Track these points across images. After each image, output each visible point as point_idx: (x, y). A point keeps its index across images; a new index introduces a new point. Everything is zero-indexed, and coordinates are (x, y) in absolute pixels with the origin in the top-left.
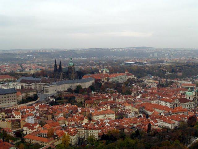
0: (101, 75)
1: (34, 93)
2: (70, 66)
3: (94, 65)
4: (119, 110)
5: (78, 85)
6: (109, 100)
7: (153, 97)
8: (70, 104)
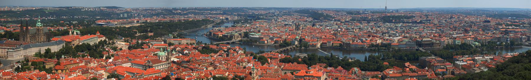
3: (64, 26)
4: (91, 76)
5: (47, 48)
6: (80, 65)
7: (124, 60)
8: (37, 71)
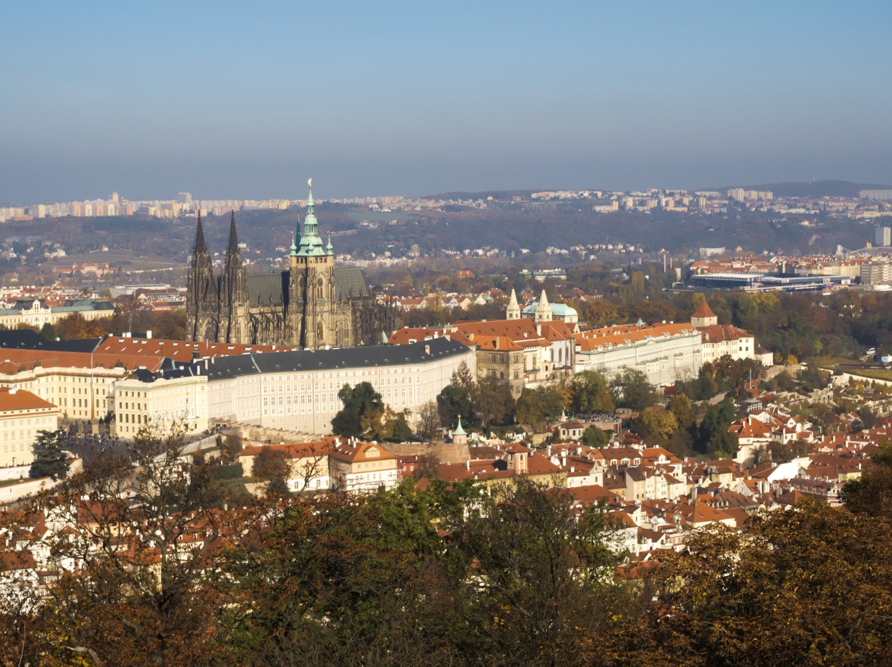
4: (645, 547)
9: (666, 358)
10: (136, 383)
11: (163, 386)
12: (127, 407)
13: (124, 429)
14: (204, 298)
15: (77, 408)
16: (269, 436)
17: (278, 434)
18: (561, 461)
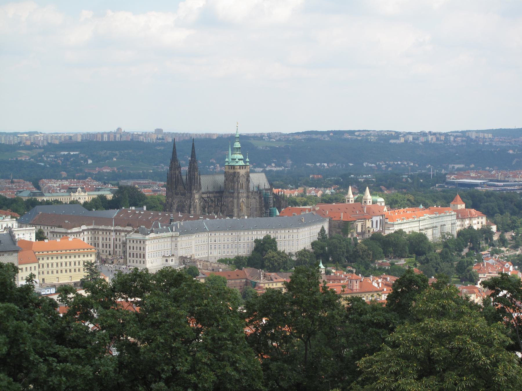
0: (353, 207)
1: (86, 259)
2: (233, 167)
9: (436, 227)
10: (139, 236)
11: (155, 238)
12: (133, 249)
13: (132, 261)
14: (176, 188)
15: (105, 249)
16: (213, 267)
17: (218, 266)
18: (379, 286)
